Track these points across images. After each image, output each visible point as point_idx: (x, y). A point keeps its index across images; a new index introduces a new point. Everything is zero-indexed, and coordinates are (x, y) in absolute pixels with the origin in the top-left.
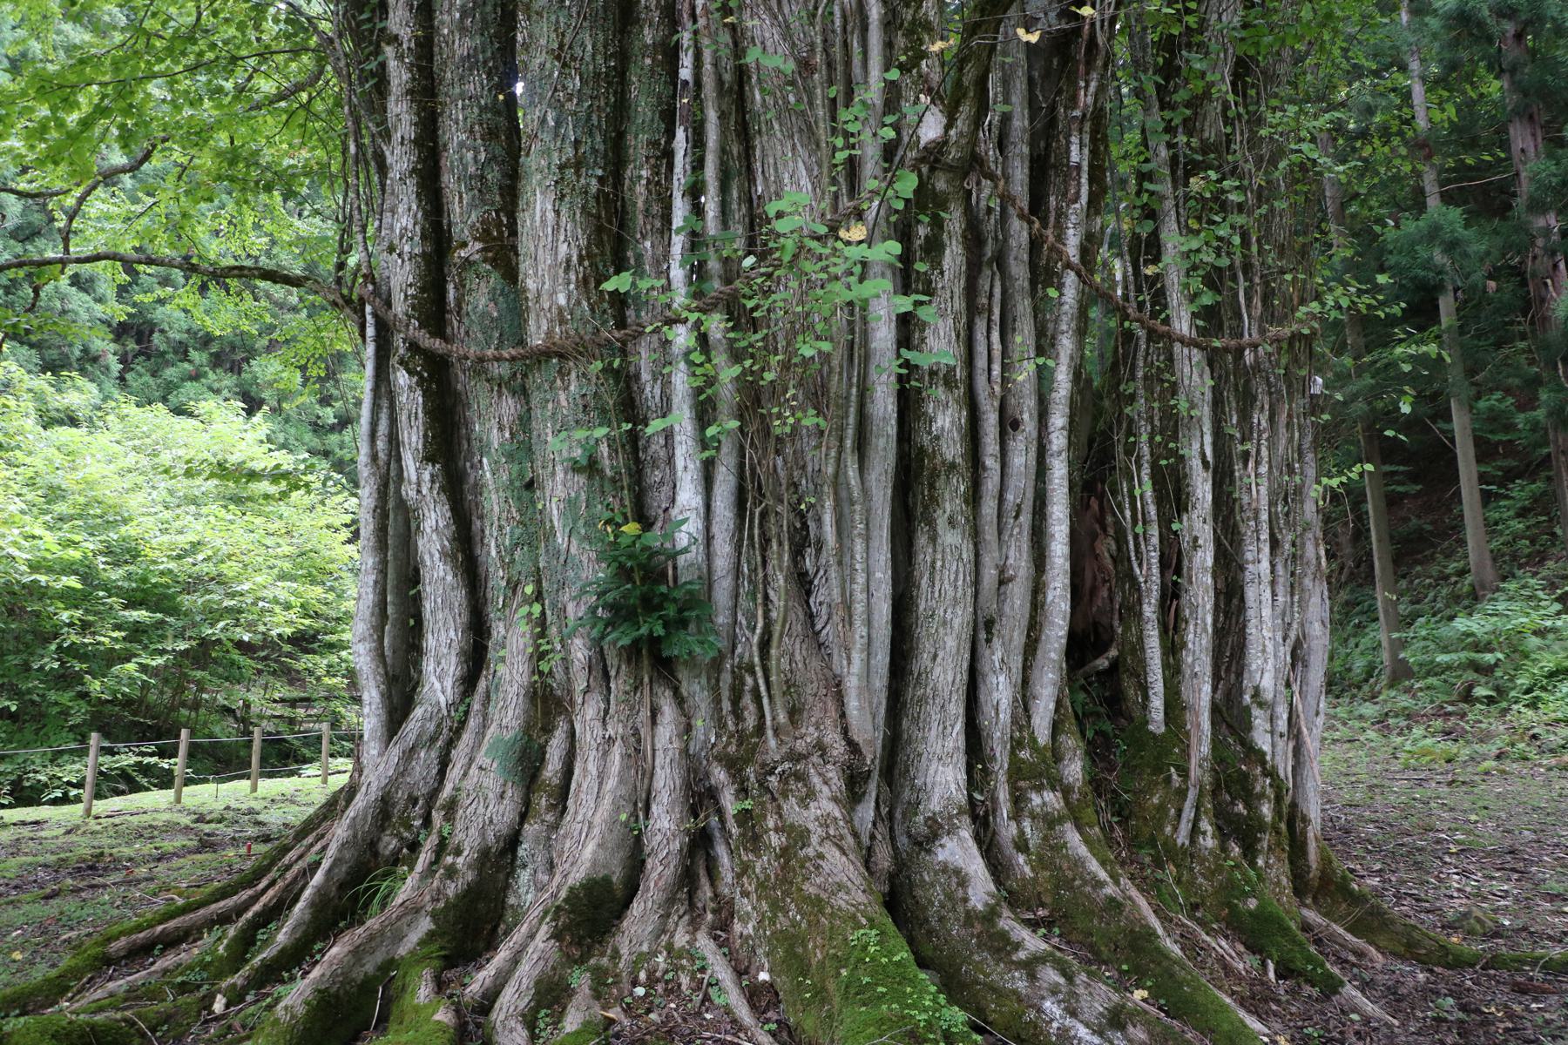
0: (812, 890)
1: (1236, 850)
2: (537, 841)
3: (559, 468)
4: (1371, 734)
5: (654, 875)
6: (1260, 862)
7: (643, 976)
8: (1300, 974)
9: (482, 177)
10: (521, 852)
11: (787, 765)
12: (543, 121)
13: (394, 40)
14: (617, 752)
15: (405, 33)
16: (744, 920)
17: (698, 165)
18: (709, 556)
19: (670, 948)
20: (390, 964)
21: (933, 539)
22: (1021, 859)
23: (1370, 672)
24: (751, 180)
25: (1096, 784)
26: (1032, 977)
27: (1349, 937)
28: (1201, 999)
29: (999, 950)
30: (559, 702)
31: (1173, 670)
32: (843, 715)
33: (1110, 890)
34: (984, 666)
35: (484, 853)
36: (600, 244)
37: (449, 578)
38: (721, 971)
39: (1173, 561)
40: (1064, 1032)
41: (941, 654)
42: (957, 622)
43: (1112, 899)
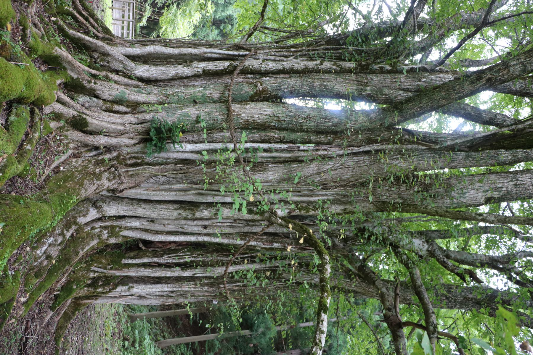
0: (85, 183)
1: (89, 282)
2: (97, 104)
3: (198, 112)
4: (114, 310)
5: (88, 138)
6: (85, 288)
7: (62, 138)
8: (56, 300)
9: (280, 90)
10: (94, 99)
11: (117, 174)
12: (291, 112)
13: (321, 64)
14: (121, 128)
15: (323, 67)
16: (76, 162)
17: (277, 150)
18: (173, 152)
19: (69, 143)
20: (65, 69)
21: (175, 209)
22: (89, 228)
24: (273, 163)
25: (108, 246)
26: (59, 235)
27: (63, 311)
28: (53, 277)
29: (66, 226)
30: (135, 109)
31: (138, 265)
32: (130, 188)
33: (81, 252)
34: (141, 220)
35: (95, 90)
36: (257, 125)
37: (170, 75)
38: (63, 158)
39: (168, 266)
40: (45, 243)
41: (145, 210)
42: (153, 215)
43: (79, 253)
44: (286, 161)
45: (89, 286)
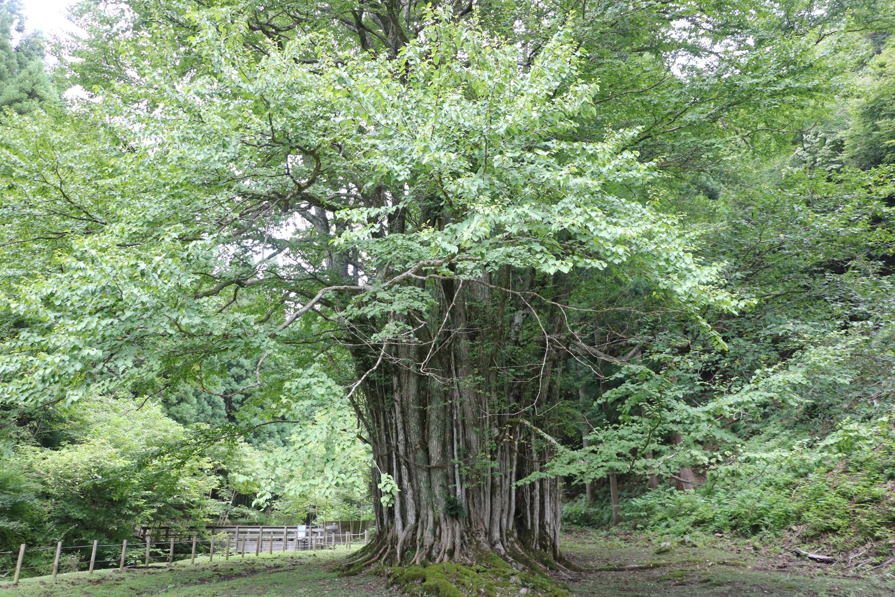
23: (609, 519)
25: (519, 538)
31: (532, 518)
39: (532, 498)
44: (464, 429)
45: (545, 551)
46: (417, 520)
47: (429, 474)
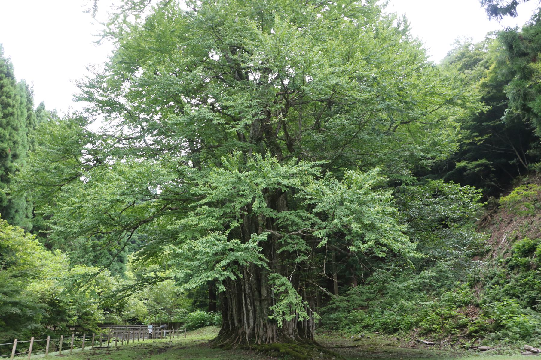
46: (254, 324)
47: (261, 303)
